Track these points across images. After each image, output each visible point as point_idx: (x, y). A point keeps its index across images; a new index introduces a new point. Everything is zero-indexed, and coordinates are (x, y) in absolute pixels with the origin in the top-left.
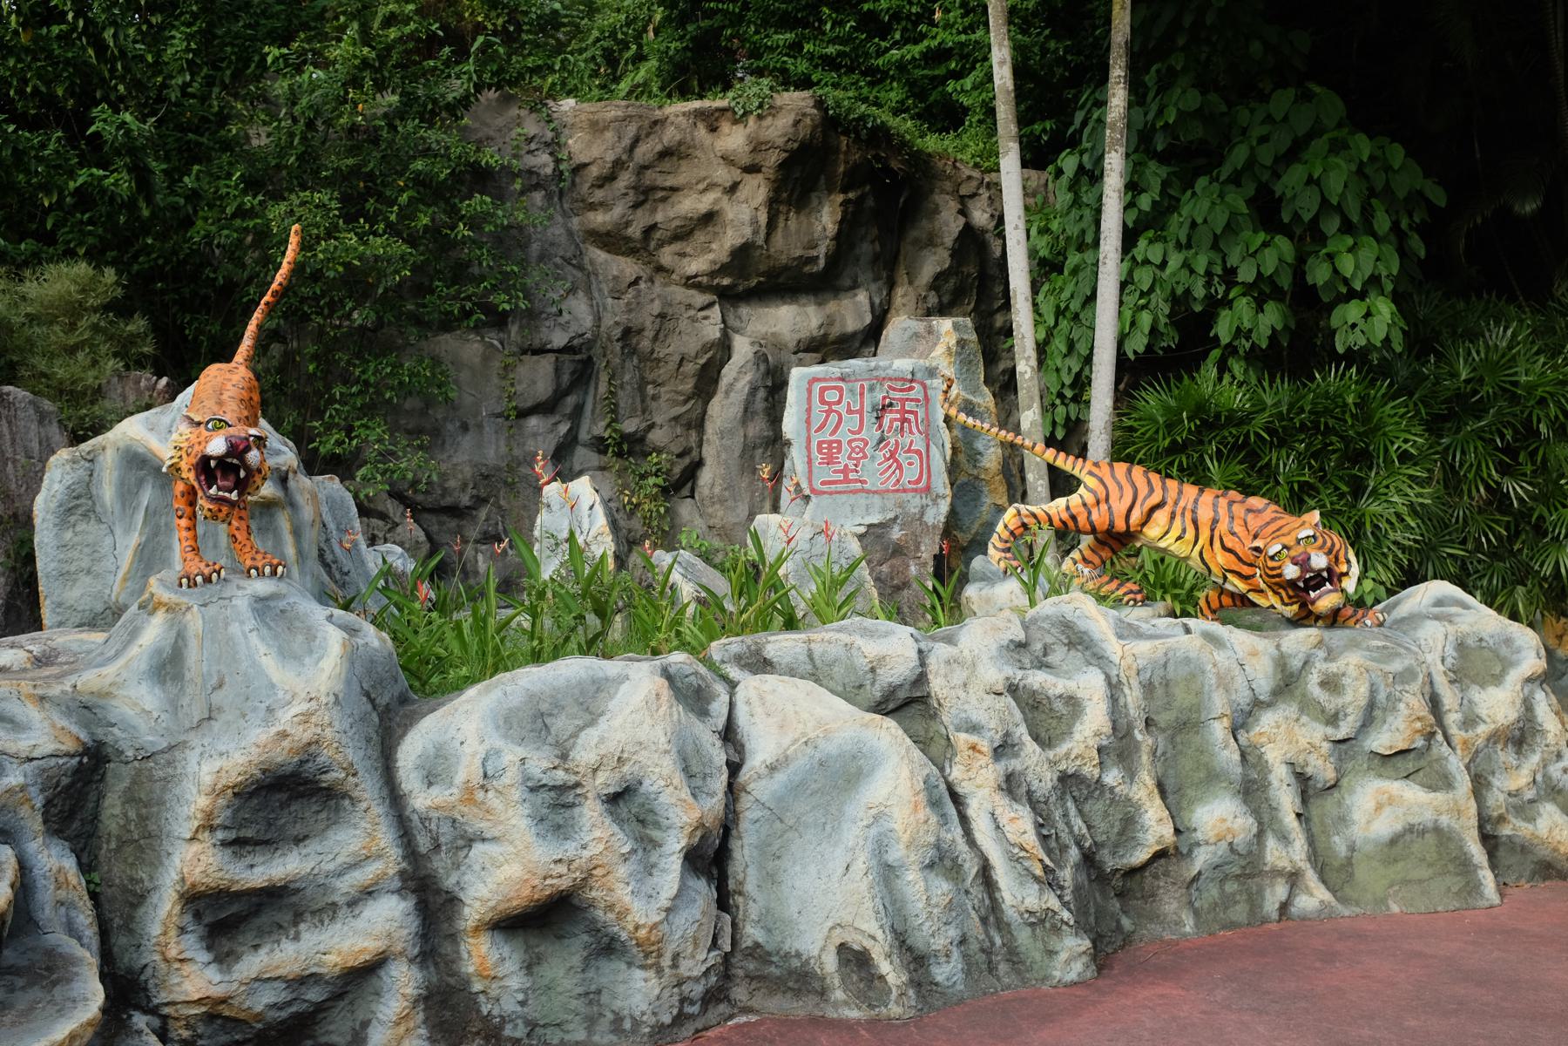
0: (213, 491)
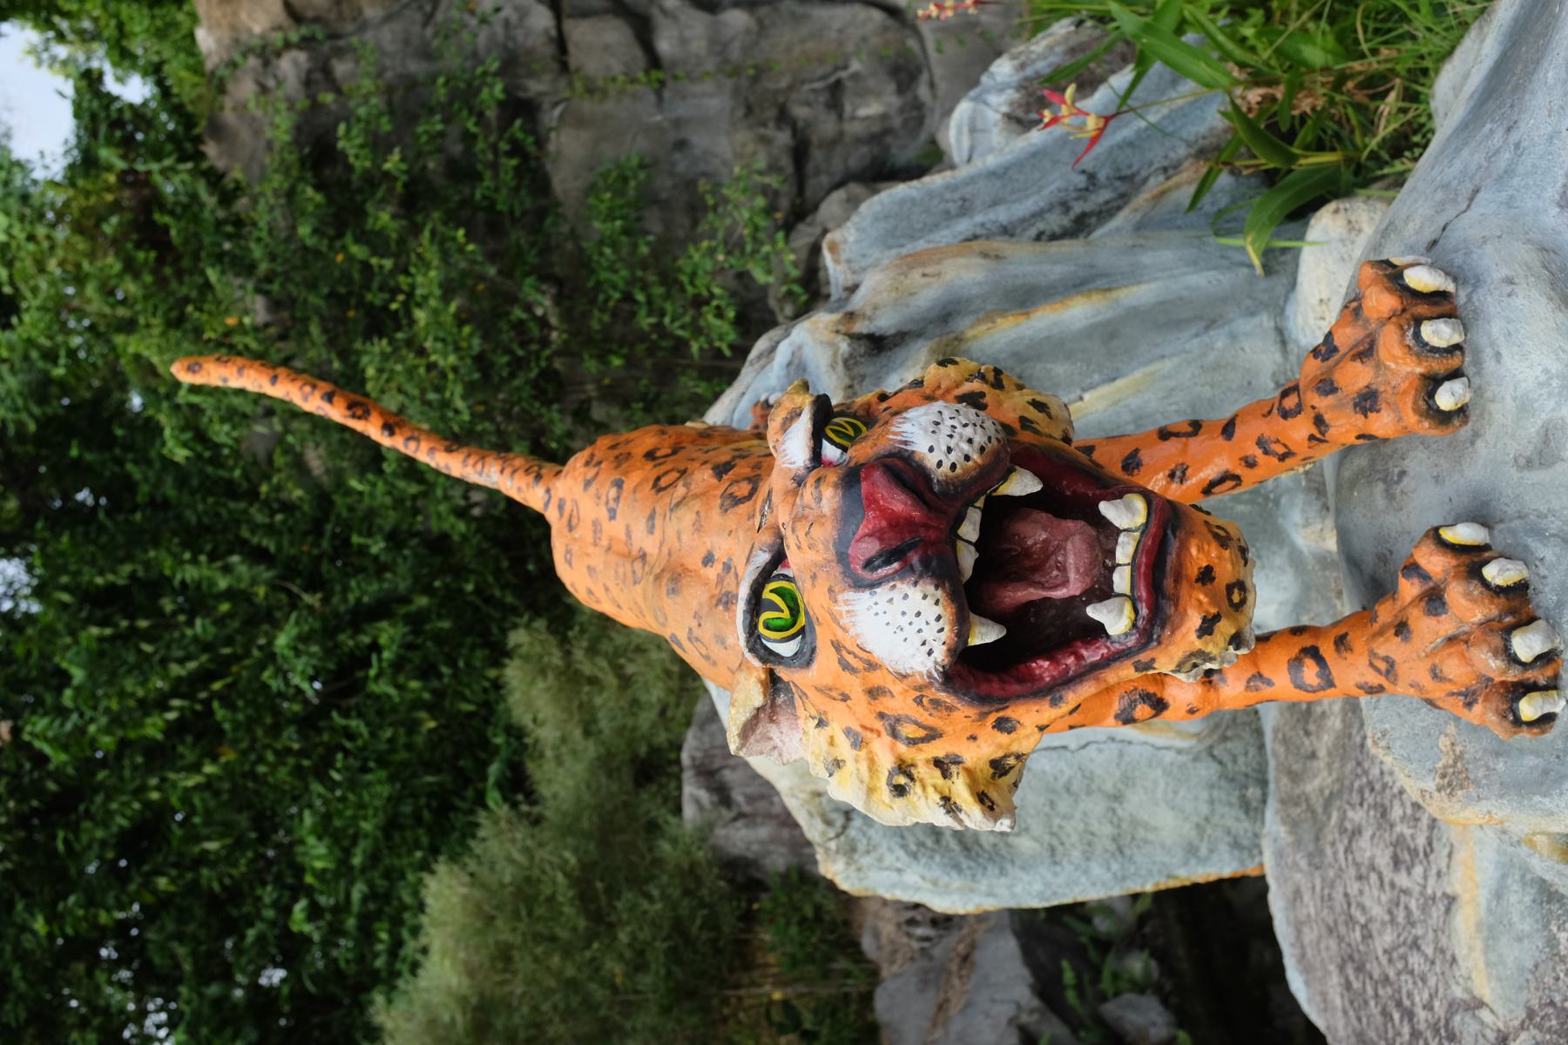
0: (1115, 619)
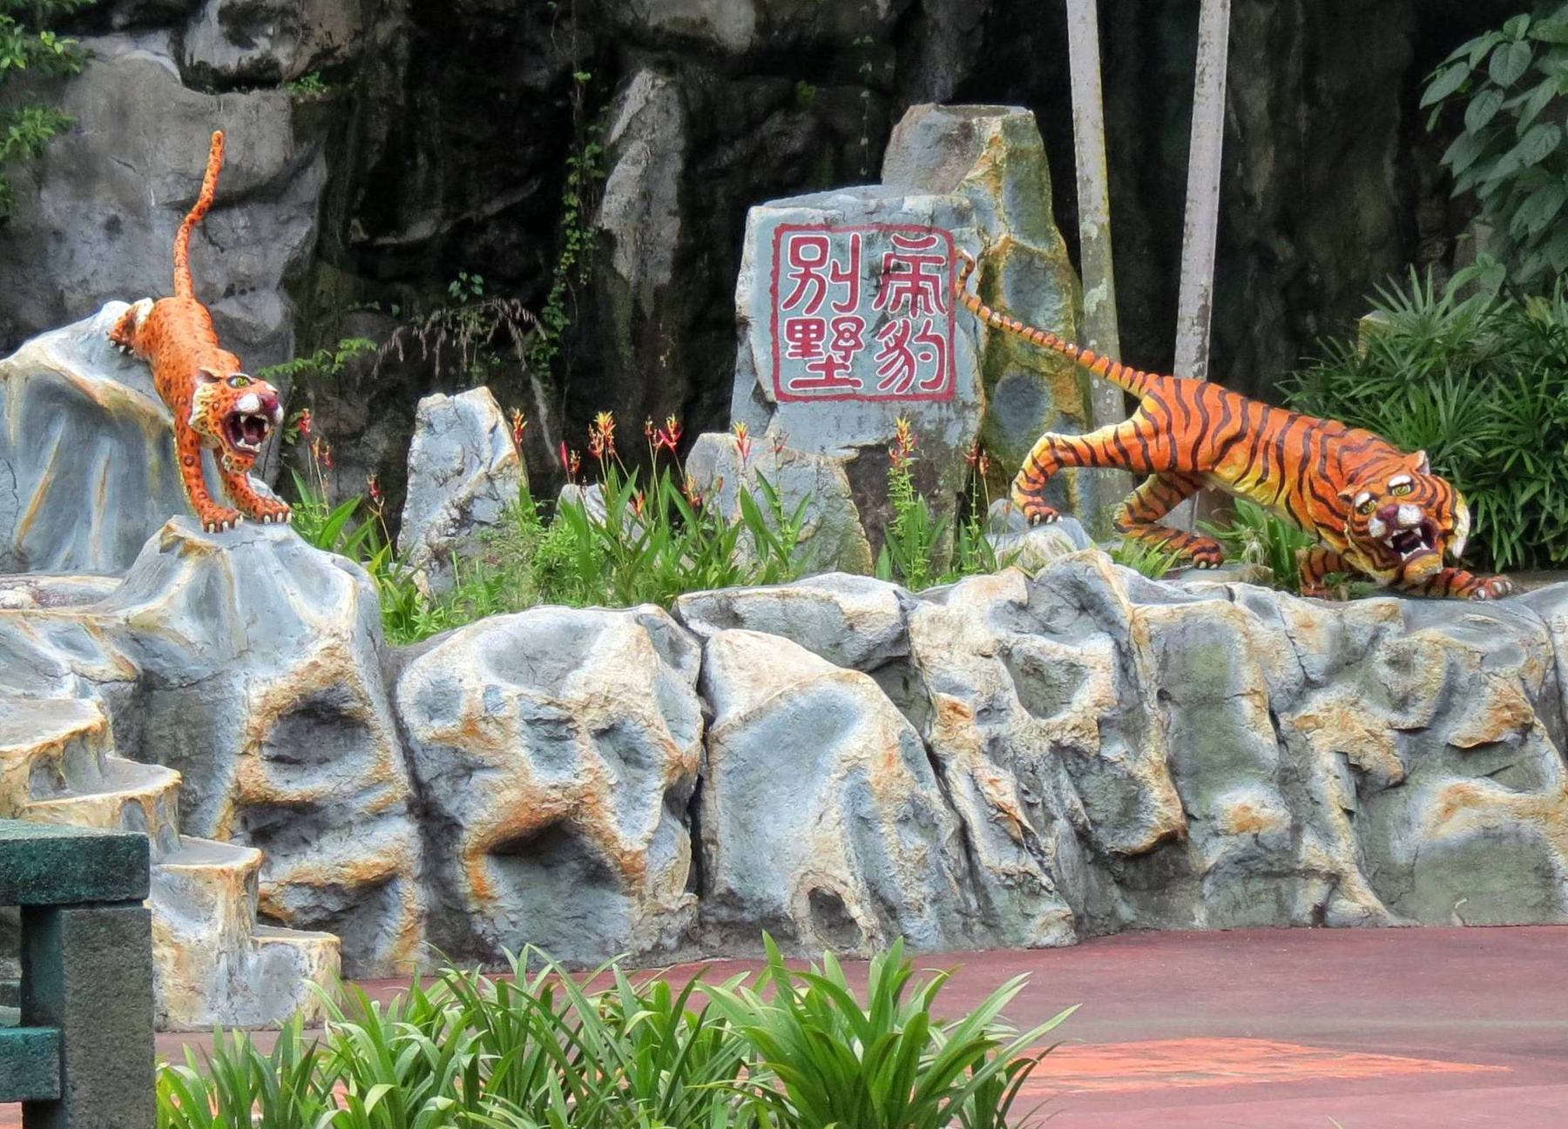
0: (241, 443)
